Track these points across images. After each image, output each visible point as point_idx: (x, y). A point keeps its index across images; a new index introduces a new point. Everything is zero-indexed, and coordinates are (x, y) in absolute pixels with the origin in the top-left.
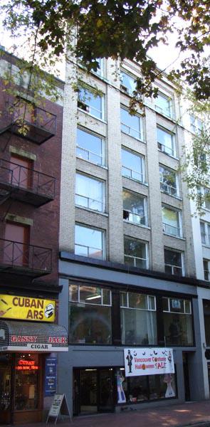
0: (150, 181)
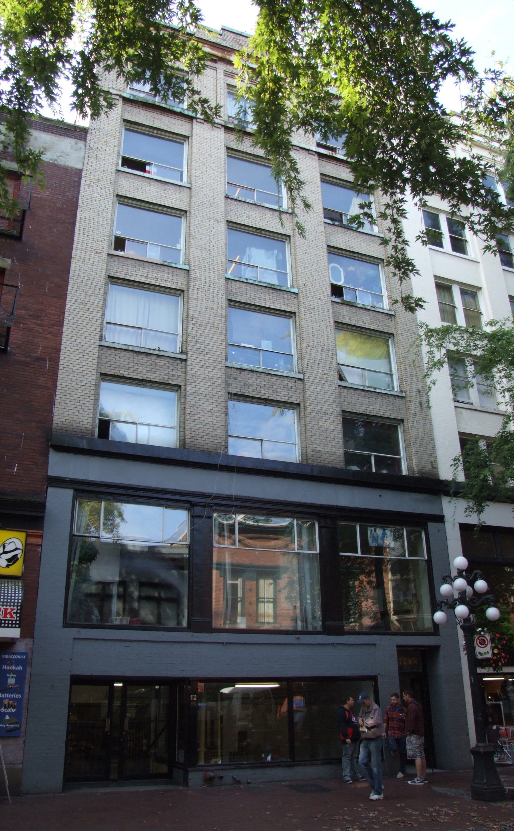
0: (300, 282)
